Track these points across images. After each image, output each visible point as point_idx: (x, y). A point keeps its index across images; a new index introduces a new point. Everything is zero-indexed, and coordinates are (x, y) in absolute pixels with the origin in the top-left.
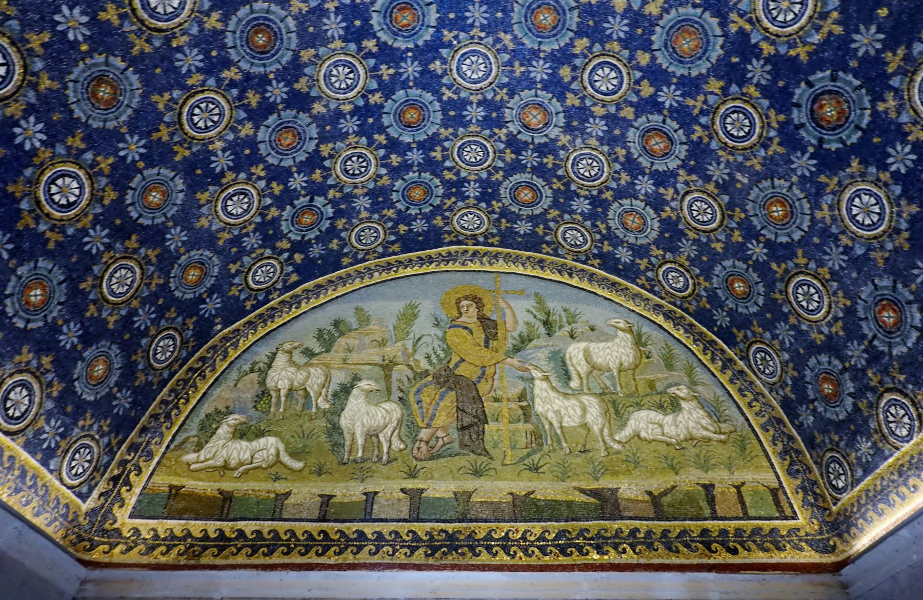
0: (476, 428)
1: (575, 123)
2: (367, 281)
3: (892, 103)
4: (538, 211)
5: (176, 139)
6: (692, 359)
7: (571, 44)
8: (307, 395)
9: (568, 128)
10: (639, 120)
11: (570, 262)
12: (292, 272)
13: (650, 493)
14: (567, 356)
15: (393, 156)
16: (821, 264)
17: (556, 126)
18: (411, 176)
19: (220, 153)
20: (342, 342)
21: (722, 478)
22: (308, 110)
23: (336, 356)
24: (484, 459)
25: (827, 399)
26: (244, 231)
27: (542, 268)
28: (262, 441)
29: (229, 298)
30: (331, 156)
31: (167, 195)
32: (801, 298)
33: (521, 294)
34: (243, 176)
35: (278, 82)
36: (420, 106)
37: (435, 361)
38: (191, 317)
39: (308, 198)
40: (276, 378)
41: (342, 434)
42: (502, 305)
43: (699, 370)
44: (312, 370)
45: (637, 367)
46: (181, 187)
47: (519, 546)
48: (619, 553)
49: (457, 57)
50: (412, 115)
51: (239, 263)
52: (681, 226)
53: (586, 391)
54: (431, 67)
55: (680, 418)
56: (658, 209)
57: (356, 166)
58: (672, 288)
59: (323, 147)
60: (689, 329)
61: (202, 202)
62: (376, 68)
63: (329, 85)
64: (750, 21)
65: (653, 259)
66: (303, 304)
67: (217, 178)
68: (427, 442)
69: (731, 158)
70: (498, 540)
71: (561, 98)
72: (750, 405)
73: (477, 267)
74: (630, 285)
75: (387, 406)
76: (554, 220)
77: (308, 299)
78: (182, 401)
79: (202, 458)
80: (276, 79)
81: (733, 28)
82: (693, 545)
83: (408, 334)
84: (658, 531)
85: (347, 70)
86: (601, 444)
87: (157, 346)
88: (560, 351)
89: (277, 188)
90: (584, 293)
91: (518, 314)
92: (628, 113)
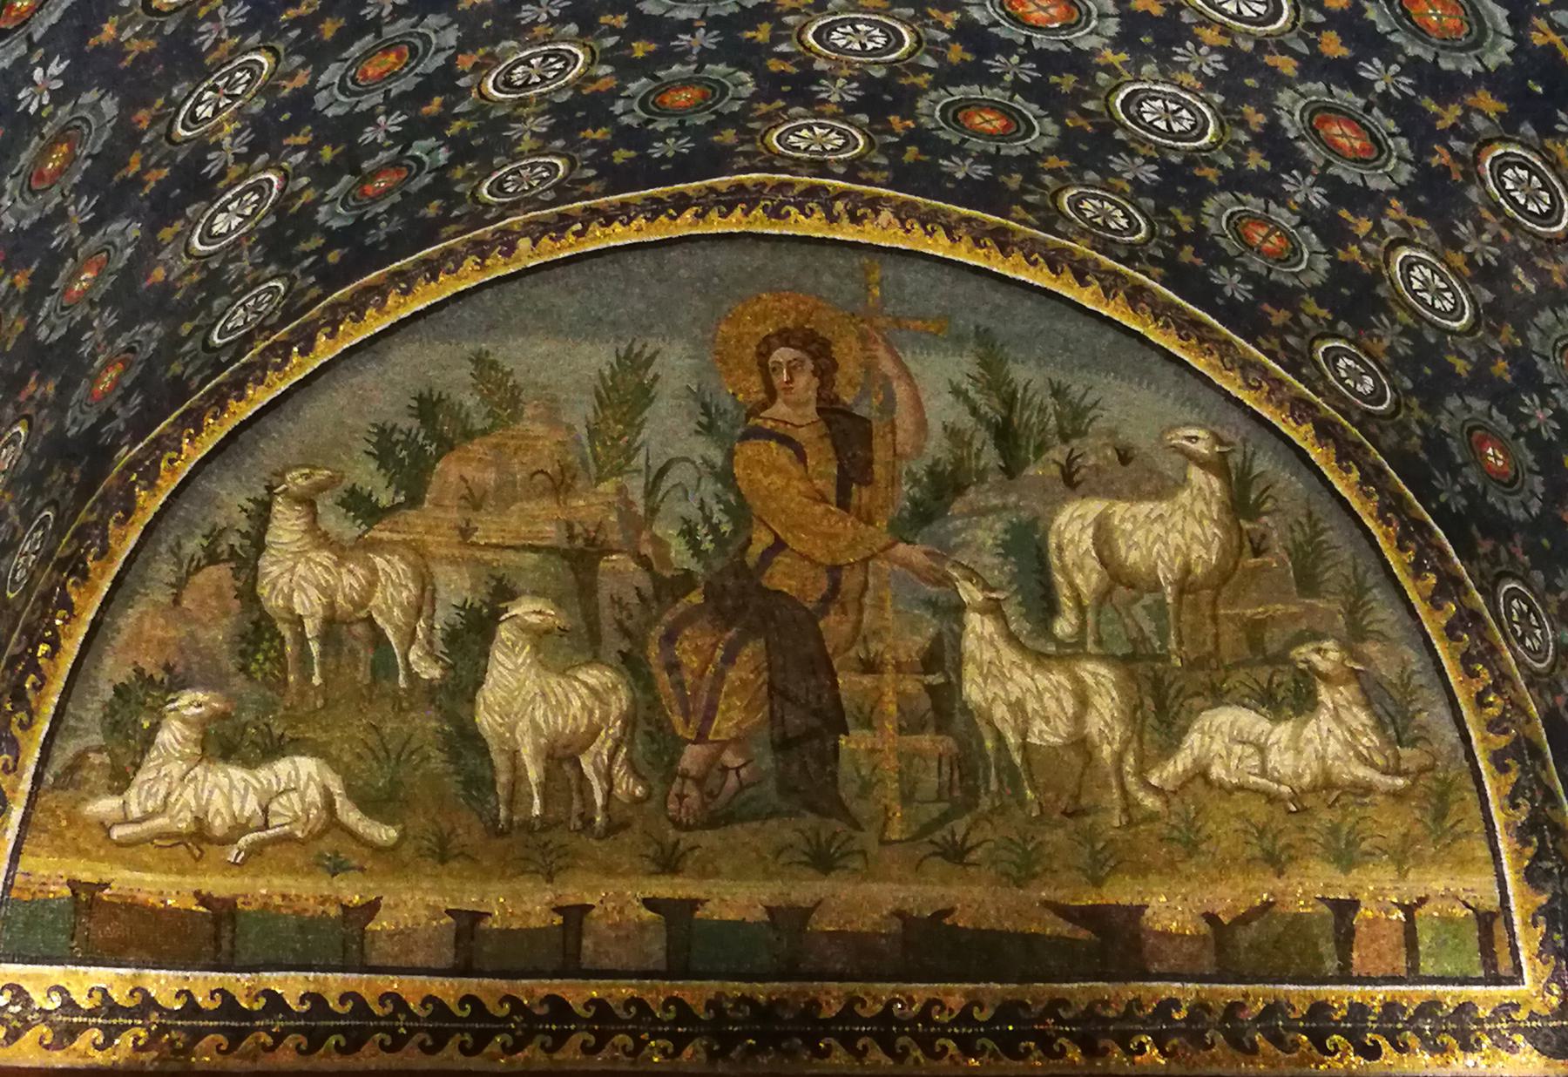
0: (816, 743)
4: (1016, 149)
6: (1367, 561)
8: (378, 638)
11: (1081, 248)
13: (1211, 918)
14: (1053, 542)
20: (450, 472)
21: (1378, 890)
24: (837, 825)
28: (283, 766)
30: (477, 67)
37: (707, 545)
41: (484, 751)
42: (887, 365)
44: (379, 561)
47: (914, 1035)
48: (1130, 1053)
52: (1382, 291)
53: (1091, 647)
55: (1310, 731)
58: (1347, 387)
60: (1371, 478)
65: (1306, 320)
70: (866, 1022)
72: (1480, 701)
75: (593, 676)
76: (1054, 172)
77: (334, 324)
78: (43, 648)
79: (135, 811)
81: (1538, 40)
82: (1290, 1037)
83: (629, 453)
86: (1116, 793)
90: (1111, 335)
91: (932, 395)
92: (1287, 65)
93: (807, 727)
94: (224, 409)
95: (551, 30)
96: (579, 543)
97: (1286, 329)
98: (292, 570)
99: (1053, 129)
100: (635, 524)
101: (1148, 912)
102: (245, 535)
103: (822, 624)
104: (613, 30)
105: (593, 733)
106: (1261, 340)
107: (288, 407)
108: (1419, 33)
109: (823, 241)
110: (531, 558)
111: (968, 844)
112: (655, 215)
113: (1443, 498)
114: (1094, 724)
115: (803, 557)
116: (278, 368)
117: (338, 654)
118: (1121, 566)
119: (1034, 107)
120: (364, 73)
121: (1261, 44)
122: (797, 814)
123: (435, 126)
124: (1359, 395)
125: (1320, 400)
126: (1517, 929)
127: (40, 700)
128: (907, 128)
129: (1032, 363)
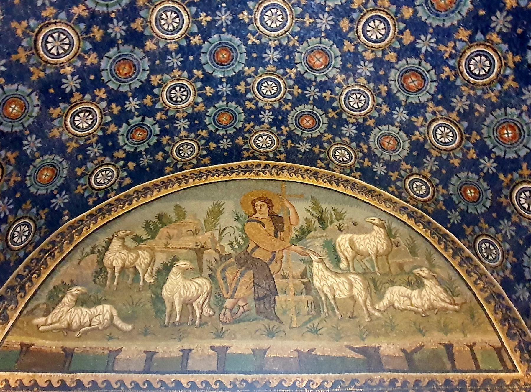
0: (268, 298)
1: (349, 65)
2: (184, 186)
5: (32, 61)
6: (430, 248)
8: (136, 271)
9: (344, 69)
10: (400, 62)
11: (338, 174)
12: (126, 177)
13: (404, 351)
14: (337, 245)
15: (207, 88)
17: (334, 67)
18: (221, 104)
19: (69, 76)
20: (164, 231)
21: (458, 340)
22: (142, 46)
23: (159, 242)
24: (276, 323)
26: (88, 142)
28: (99, 308)
29: (75, 195)
30: (159, 86)
31: (24, 108)
32: (523, 201)
33: (301, 197)
34: (88, 97)
35: (118, 21)
36: (231, 49)
37: (236, 247)
38: (44, 209)
39: (140, 118)
40: (111, 258)
42: (287, 205)
43: (436, 256)
44: (140, 252)
45: (389, 253)
46: (36, 102)
49: (261, 9)
50: (223, 56)
51: (84, 168)
52: (426, 147)
53: (352, 271)
54: (240, 16)
55: (424, 292)
56: (409, 133)
57: (179, 94)
59: (153, 78)
60: (427, 225)
61: (54, 116)
62: (197, 15)
63: (159, 26)
65: (402, 172)
66: (134, 202)
67: (67, 97)
68: (231, 310)
69: (472, 92)
71: (340, 45)
72: (475, 283)
73: (268, 176)
75: (199, 281)
76: (328, 142)
77: (138, 198)
78: (35, 275)
79: (49, 321)
80: (116, 18)
83: (215, 226)
84: (412, 382)
85: (174, 15)
86: (365, 312)
87: (14, 231)
88: (331, 241)
89: (116, 109)
91: (300, 211)
92: (391, 57)
94: (104, 217)
95: (179, 73)
96: (199, 247)
101: (382, 349)
102: (104, 247)
103: (270, 266)
104: (198, 79)
106: (390, 189)
107: (122, 217)
111: (318, 328)
112: (226, 174)
113: (452, 221)
116: (122, 208)
117: (123, 276)
118: (359, 250)
119: (319, 110)
120: (119, 70)
122: (262, 320)
125: (408, 205)
126: (510, 353)
127: (30, 290)
128: (286, 131)
129: (327, 203)
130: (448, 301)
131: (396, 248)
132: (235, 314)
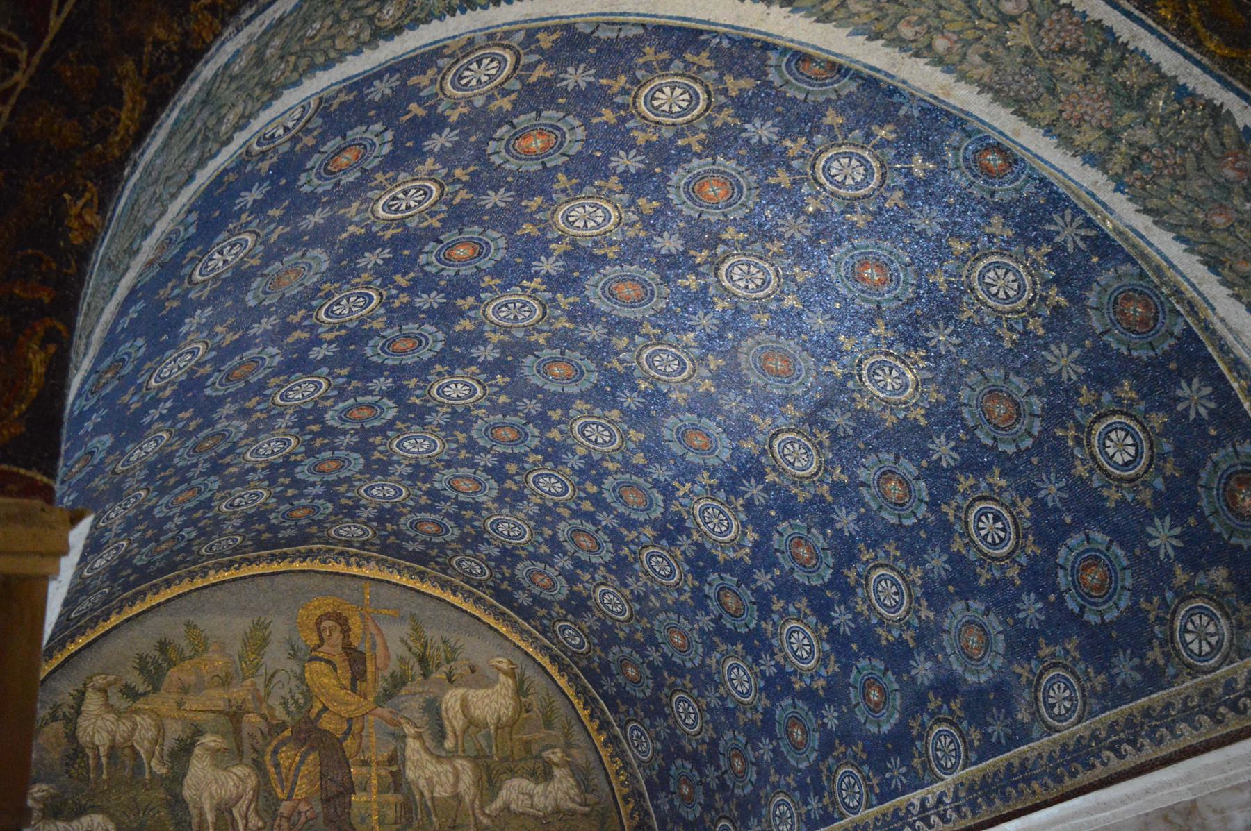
2: (199, 582)
3: (770, 627)
7: (526, 454)
8: (136, 754)
9: (499, 499)
11: (457, 581)
14: (443, 707)
16: (701, 695)
20: (173, 675)
25: (683, 798)
27: (422, 579)
37: (292, 708)
40: (90, 729)
44: (138, 719)
52: (589, 603)
53: (460, 753)
55: (550, 788)
60: (573, 679)
64: (688, 513)
65: (554, 614)
73: (341, 568)
74: (521, 621)
75: (240, 771)
81: (673, 509)
86: (471, 819)
88: (435, 700)
90: (467, 618)
91: (391, 644)
92: (565, 512)
93: (337, 795)
97: (544, 617)
98: (94, 724)
99: (457, 532)
100: (258, 699)
102: (72, 707)
105: (239, 798)
107: (95, 646)
108: (625, 504)
109: (344, 575)
110: (211, 716)
114: (462, 787)
115: (335, 714)
116: (92, 628)
117: (115, 764)
121: (556, 504)
123: (194, 523)
124: (573, 646)
130: (578, 800)
131: (525, 715)
132: (294, 825)
